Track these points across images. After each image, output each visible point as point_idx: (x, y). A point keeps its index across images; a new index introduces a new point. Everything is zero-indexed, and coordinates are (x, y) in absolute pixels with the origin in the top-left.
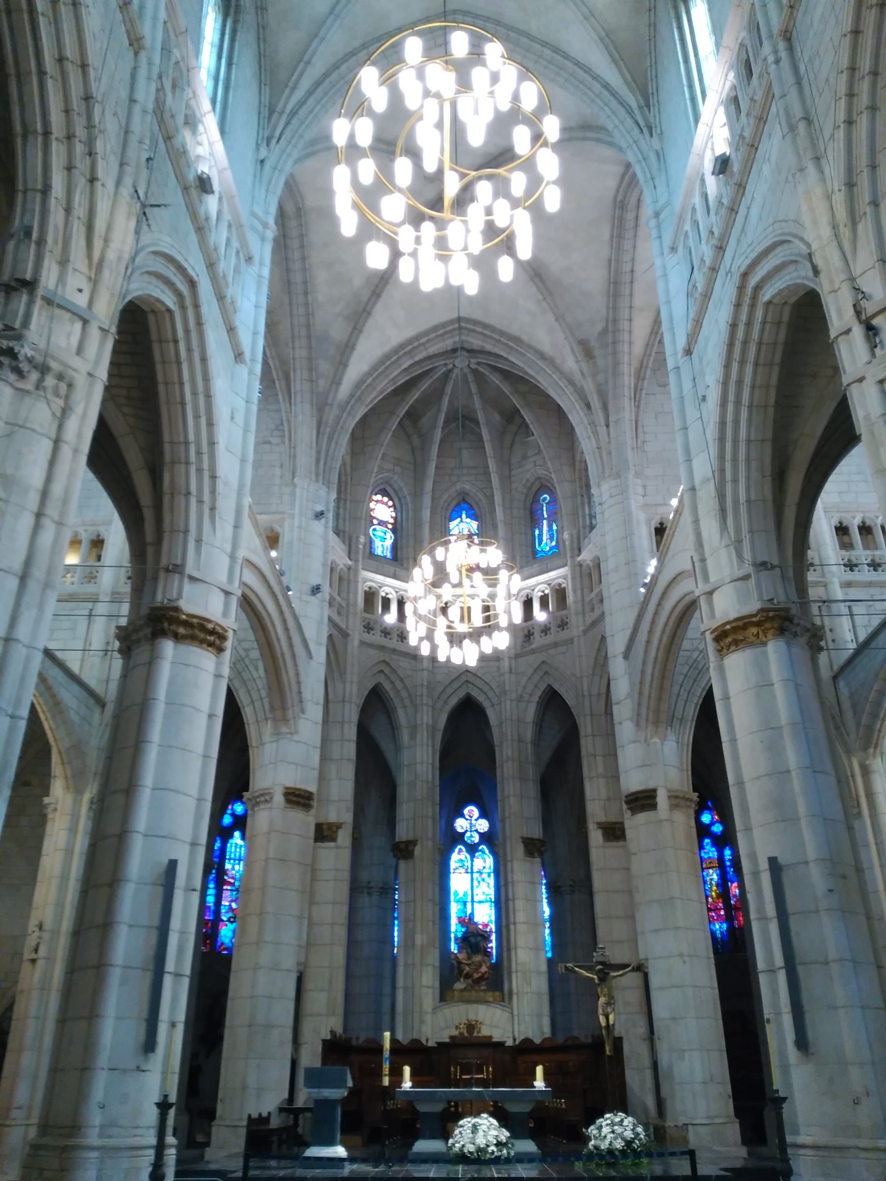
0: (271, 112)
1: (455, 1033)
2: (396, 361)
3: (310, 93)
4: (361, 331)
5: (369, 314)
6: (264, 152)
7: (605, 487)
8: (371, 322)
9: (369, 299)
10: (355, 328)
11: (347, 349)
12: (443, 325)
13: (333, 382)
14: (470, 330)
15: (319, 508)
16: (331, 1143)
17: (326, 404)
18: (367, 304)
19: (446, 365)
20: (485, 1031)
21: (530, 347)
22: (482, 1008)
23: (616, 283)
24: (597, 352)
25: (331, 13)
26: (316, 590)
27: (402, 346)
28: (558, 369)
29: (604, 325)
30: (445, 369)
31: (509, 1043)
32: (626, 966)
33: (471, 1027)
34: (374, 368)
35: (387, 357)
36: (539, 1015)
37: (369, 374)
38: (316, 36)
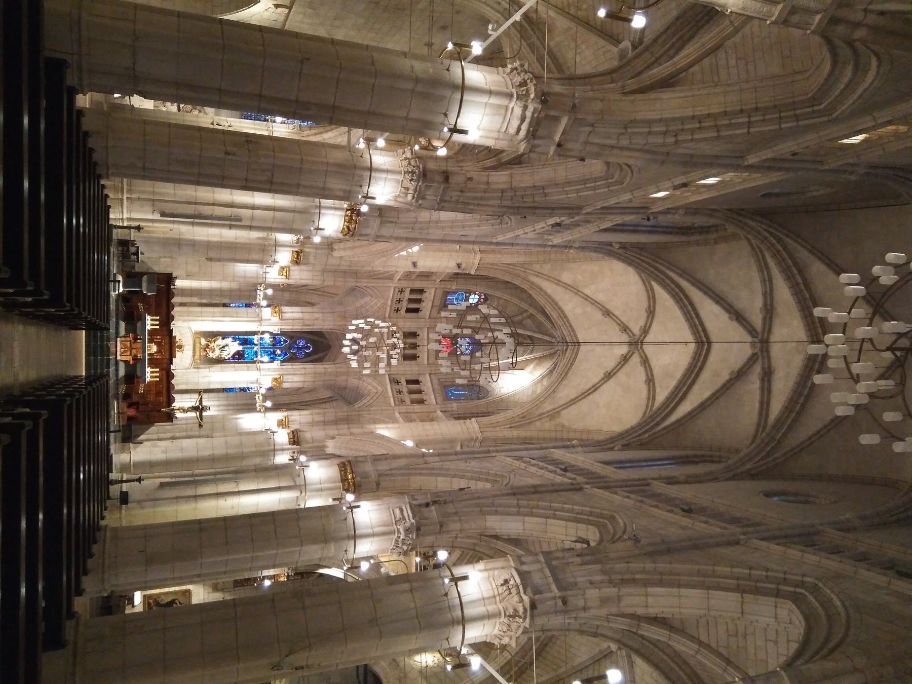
0: (641, 249)
1: (177, 339)
6: (617, 246)
7: (476, 426)
11: (558, 282)
12: (576, 336)
15: (463, 266)
16: (123, 286)
20: (178, 354)
22: (191, 353)
26: (415, 264)
27: (562, 311)
31: (172, 367)
32: (201, 420)
33: (180, 347)
34: (549, 297)
36: (187, 384)
37: (546, 293)
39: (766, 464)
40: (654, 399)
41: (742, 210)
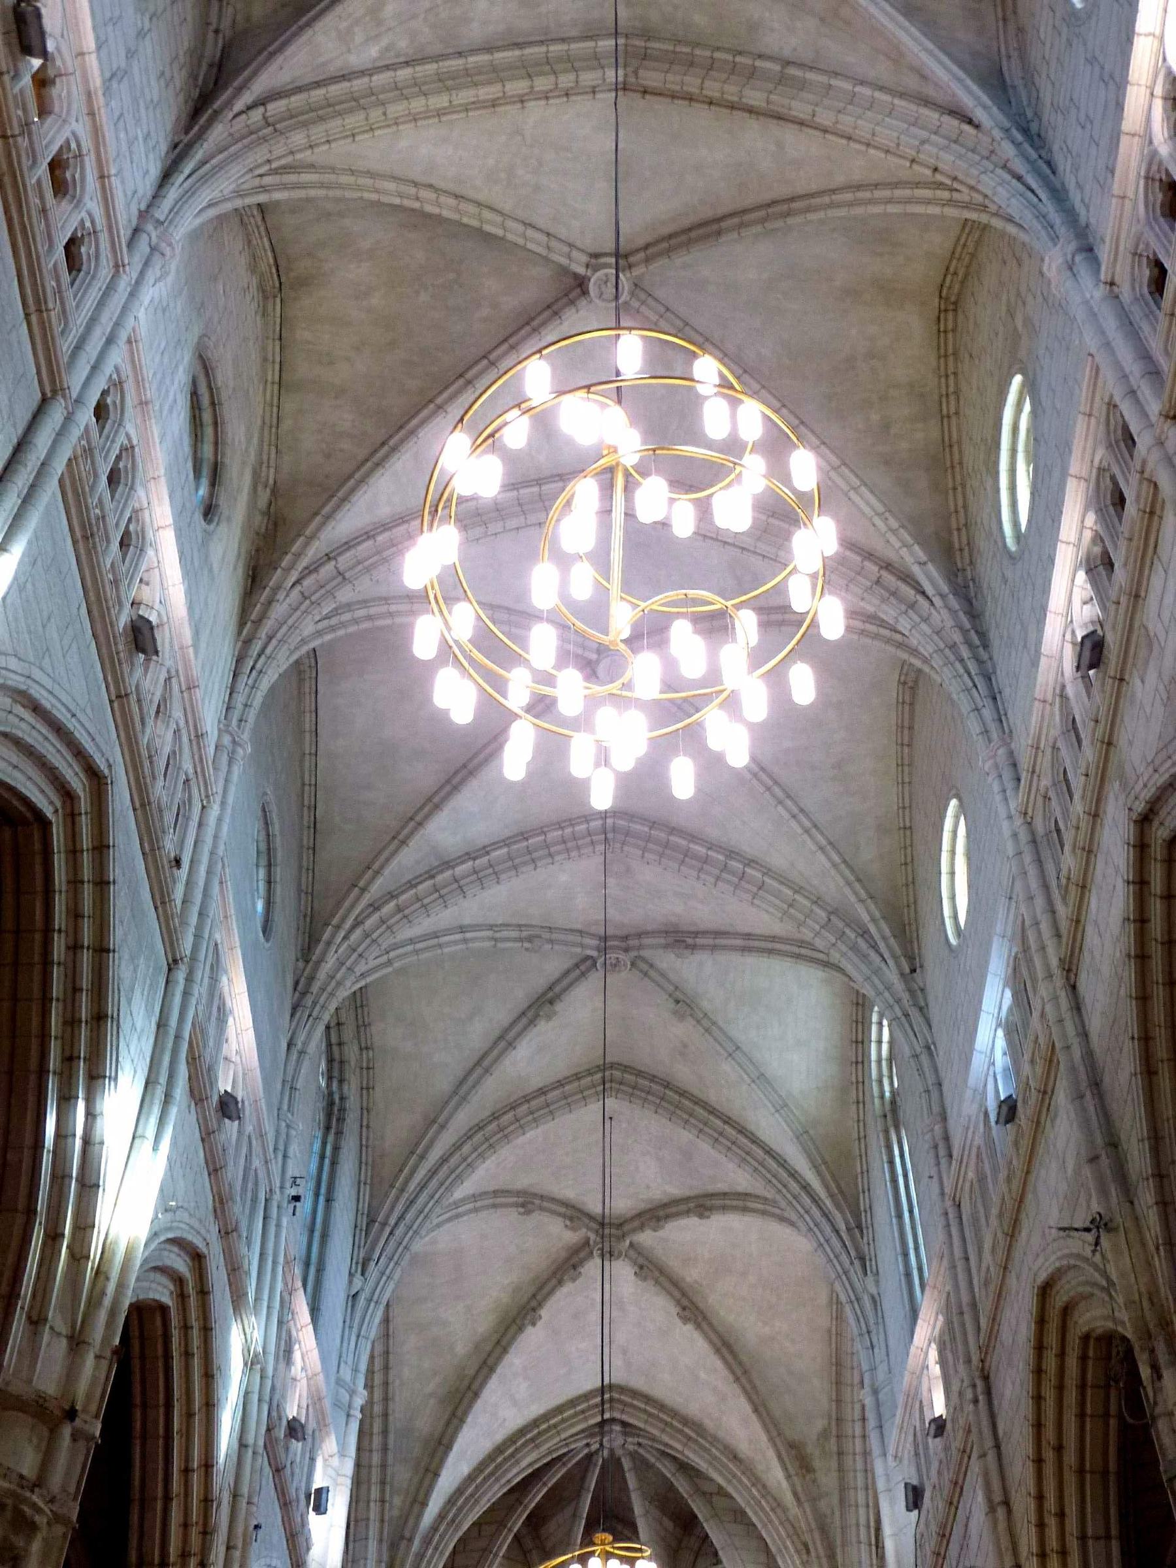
0: (371, 1221)
2: (512, 1455)
3: (422, 1187)
4: (462, 1421)
5: (476, 1395)
6: (358, 1282)
8: (479, 1405)
9: (478, 1372)
10: (453, 1414)
13: (415, 1501)
14: (625, 1404)
17: (402, 1537)
18: (475, 1377)
19: (588, 1445)
21: (714, 1440)
23: (838, 1364)
24: (817, 1464)
25: (455, 1093)
27: (522, 1432)
28: (757, 1481)
29: (826, 1422)
30: (586, 1451)
35: (499, 1450)
37: (470, 1478)
38: (434, 1121)
39: (884, 938)
40: (746, 1196)
41: (297, 983)
